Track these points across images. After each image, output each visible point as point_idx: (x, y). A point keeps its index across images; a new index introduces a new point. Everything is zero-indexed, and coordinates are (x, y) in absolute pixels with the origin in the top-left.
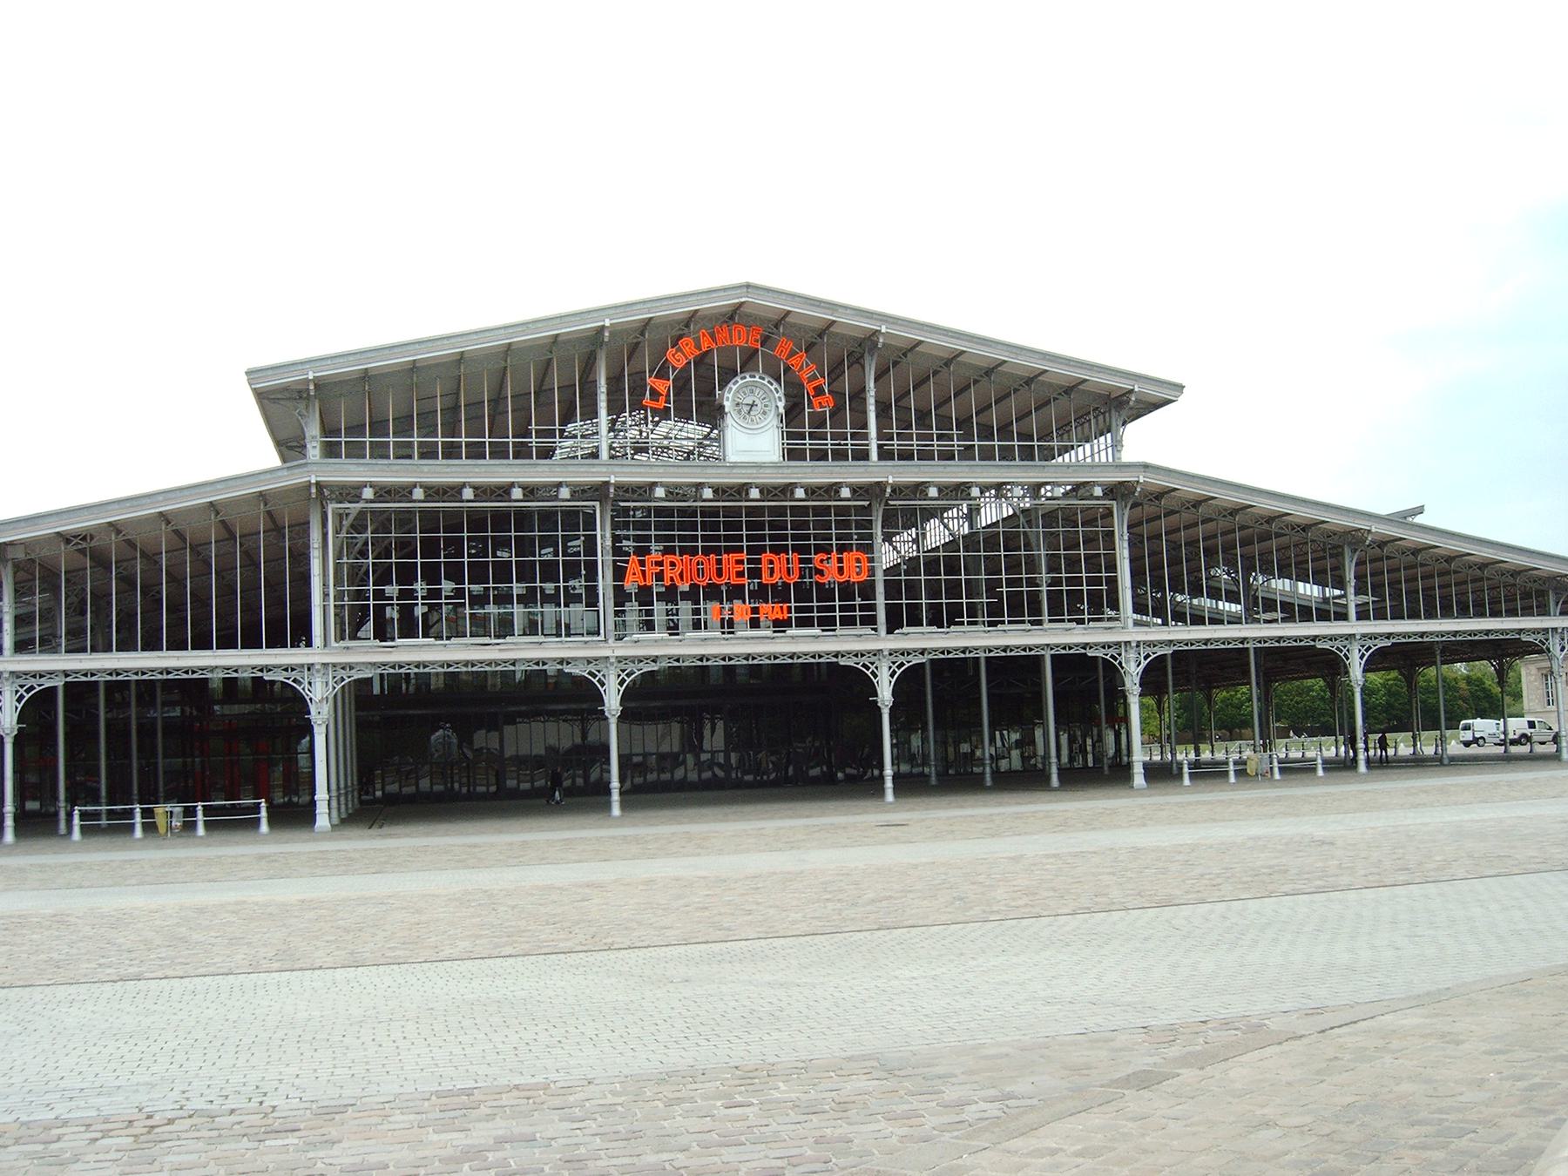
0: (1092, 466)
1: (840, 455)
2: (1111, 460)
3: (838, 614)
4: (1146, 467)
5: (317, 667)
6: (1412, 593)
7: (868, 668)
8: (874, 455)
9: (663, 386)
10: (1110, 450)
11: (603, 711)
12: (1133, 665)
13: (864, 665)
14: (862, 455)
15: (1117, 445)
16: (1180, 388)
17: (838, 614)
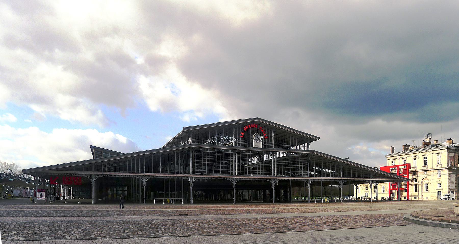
0: (305, 150)
1: (268, 147)
2: (307, 149)
3: (282, 173)
4: (314, 151)
5: (93, 175)
6: (348, 173)
7: (271, 181)
8: (273, 147)
9: (243, 134)
10: (307, 147)
11: (233, 186)
12: (309, 183)
13: (271, 181)
14: (271, 147)
15: (308, 147)
16: (319, 138)
17: (282, 173)
